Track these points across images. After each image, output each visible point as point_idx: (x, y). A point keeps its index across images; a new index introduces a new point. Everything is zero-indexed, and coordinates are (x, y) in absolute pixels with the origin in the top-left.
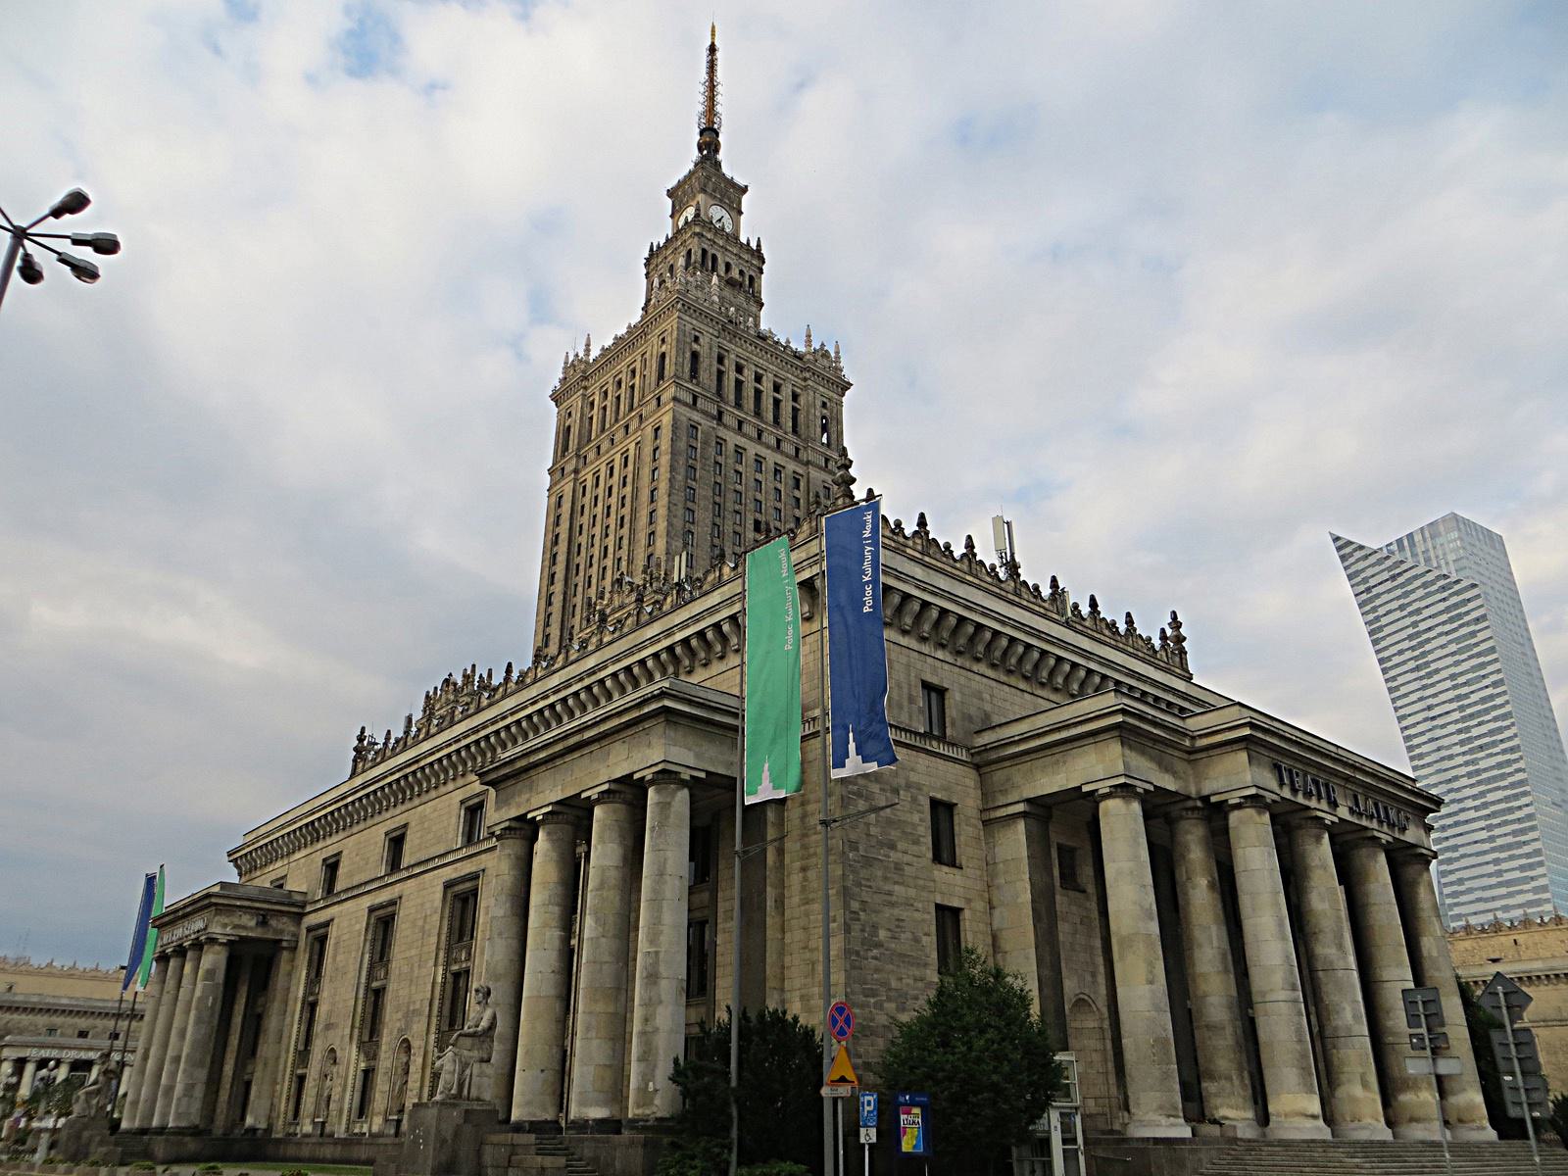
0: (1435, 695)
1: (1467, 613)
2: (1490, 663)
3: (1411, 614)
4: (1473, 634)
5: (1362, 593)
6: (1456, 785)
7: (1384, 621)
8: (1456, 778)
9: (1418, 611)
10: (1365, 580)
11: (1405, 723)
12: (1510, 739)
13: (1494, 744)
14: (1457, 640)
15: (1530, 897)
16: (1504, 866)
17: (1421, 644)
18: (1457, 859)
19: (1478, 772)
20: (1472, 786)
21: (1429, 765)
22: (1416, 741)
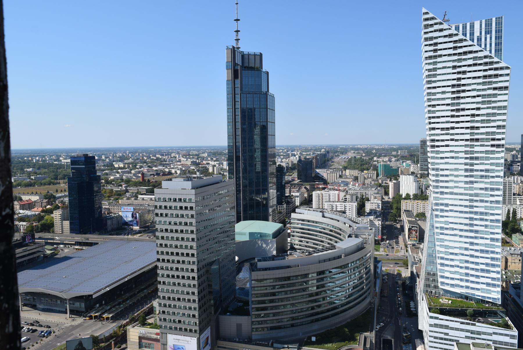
0: (458, 122)
1: (496, 82)
3: (459, 73)
4: (495, 95)
5: (430, 51)
6: (456, 173)
7: (439, 72)
8: (456, 170)
9: (464, 72)
10: (436, 44)
11: (433, 132)
12: (497, 158)
13: (487, 158)
14: (483, 96)
15: (488, 242)
16: (475, 222)
17: (458, 92)
18: (447, 211)
19: (472, 170)
20: (466, 176)
21: (442, 158)
22: (437, 144)
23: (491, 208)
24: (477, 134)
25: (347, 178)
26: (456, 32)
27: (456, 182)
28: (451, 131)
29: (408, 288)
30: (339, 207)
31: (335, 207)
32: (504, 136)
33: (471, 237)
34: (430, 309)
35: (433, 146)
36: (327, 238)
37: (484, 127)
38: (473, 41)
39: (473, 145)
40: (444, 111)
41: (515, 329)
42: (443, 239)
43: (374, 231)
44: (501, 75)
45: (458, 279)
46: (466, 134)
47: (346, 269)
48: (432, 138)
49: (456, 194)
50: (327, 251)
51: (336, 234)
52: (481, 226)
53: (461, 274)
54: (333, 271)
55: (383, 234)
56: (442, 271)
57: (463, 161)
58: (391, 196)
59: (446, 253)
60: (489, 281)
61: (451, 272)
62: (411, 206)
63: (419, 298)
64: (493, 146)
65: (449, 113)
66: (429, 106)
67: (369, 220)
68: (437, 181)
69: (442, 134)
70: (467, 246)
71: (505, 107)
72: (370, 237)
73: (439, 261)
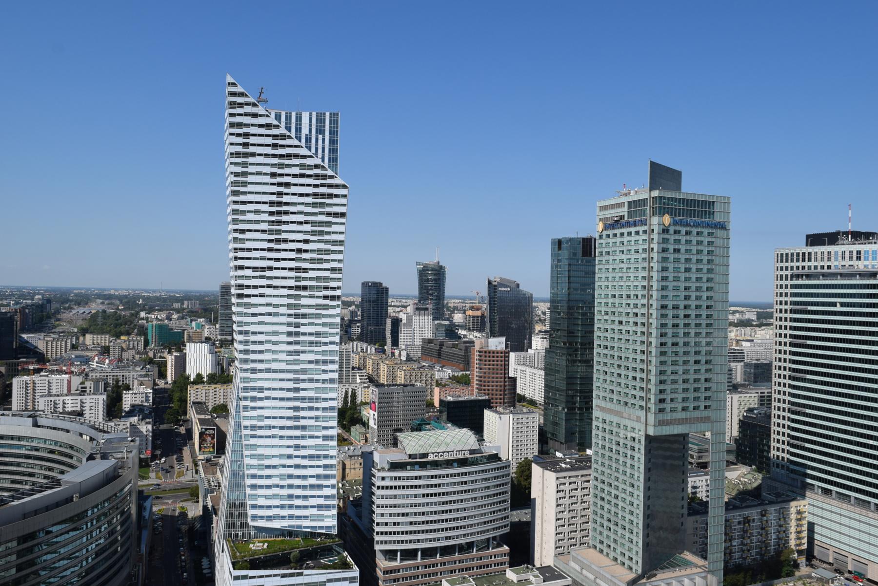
0: (277, 260)
1: (330, 205)
2: (334, 252)
3: (280, 184)
4: (329, 224)
5: (237, 144)
6: (274, 338)
7: (250, 179)
8: (275, 333)
9: (287, 185)
10: (246, 135)
11: (240, 273)
12: (332, 316)
13: (318, 316)
14: (313, 223)
15: (319, 441)
16: (302, 414)
17: (279, 213)
18: (261, 399)
19: (297, 334)
20: (289, 343)
21: (254, 315)
22: (246, 291)
23: (324, 391)
24: (305, 279)
25: (87, 350)
26: (275, 123)
27: (275, 352)
28: (268, 273)
29: (198, 536)
30: (70, 405)
31: (61, 406)
32: (339, 284)
33: (297, 438)
34: (235, 565)
35: (240, 296)
36: (41, 466)
37: (314, 269)
38: (300, 141)
39: (299, 295)
40: (257, 241)
41: (356, 568)
42: (255, 445)
43: (137, 443)
44: (337, 196)
45: (277, 507)
46: (289, 278)
47: (83, 521)
48: (240, 282)
49: (275, 371)
50: (42, 491)
51: (63, 457)
52: (310, 418)
53: (281, 497)
54: (54, 529)
55: (154, 447)
56: (254, 497)
57: (285, 319)
58: (170, 378)
59: (260, 467)
60: (321, 501)
61: (267, 497)
62: (204, 395)
63: (217, 549)
64: (325, 297)
65: (266, 245)
66: (236, 231)
67: (128, 425)
68: (246, 352)
69: (254, 277)
70: (291, 451)
71: (341, 243)
72: (130, 455)
73: (249, 482)
